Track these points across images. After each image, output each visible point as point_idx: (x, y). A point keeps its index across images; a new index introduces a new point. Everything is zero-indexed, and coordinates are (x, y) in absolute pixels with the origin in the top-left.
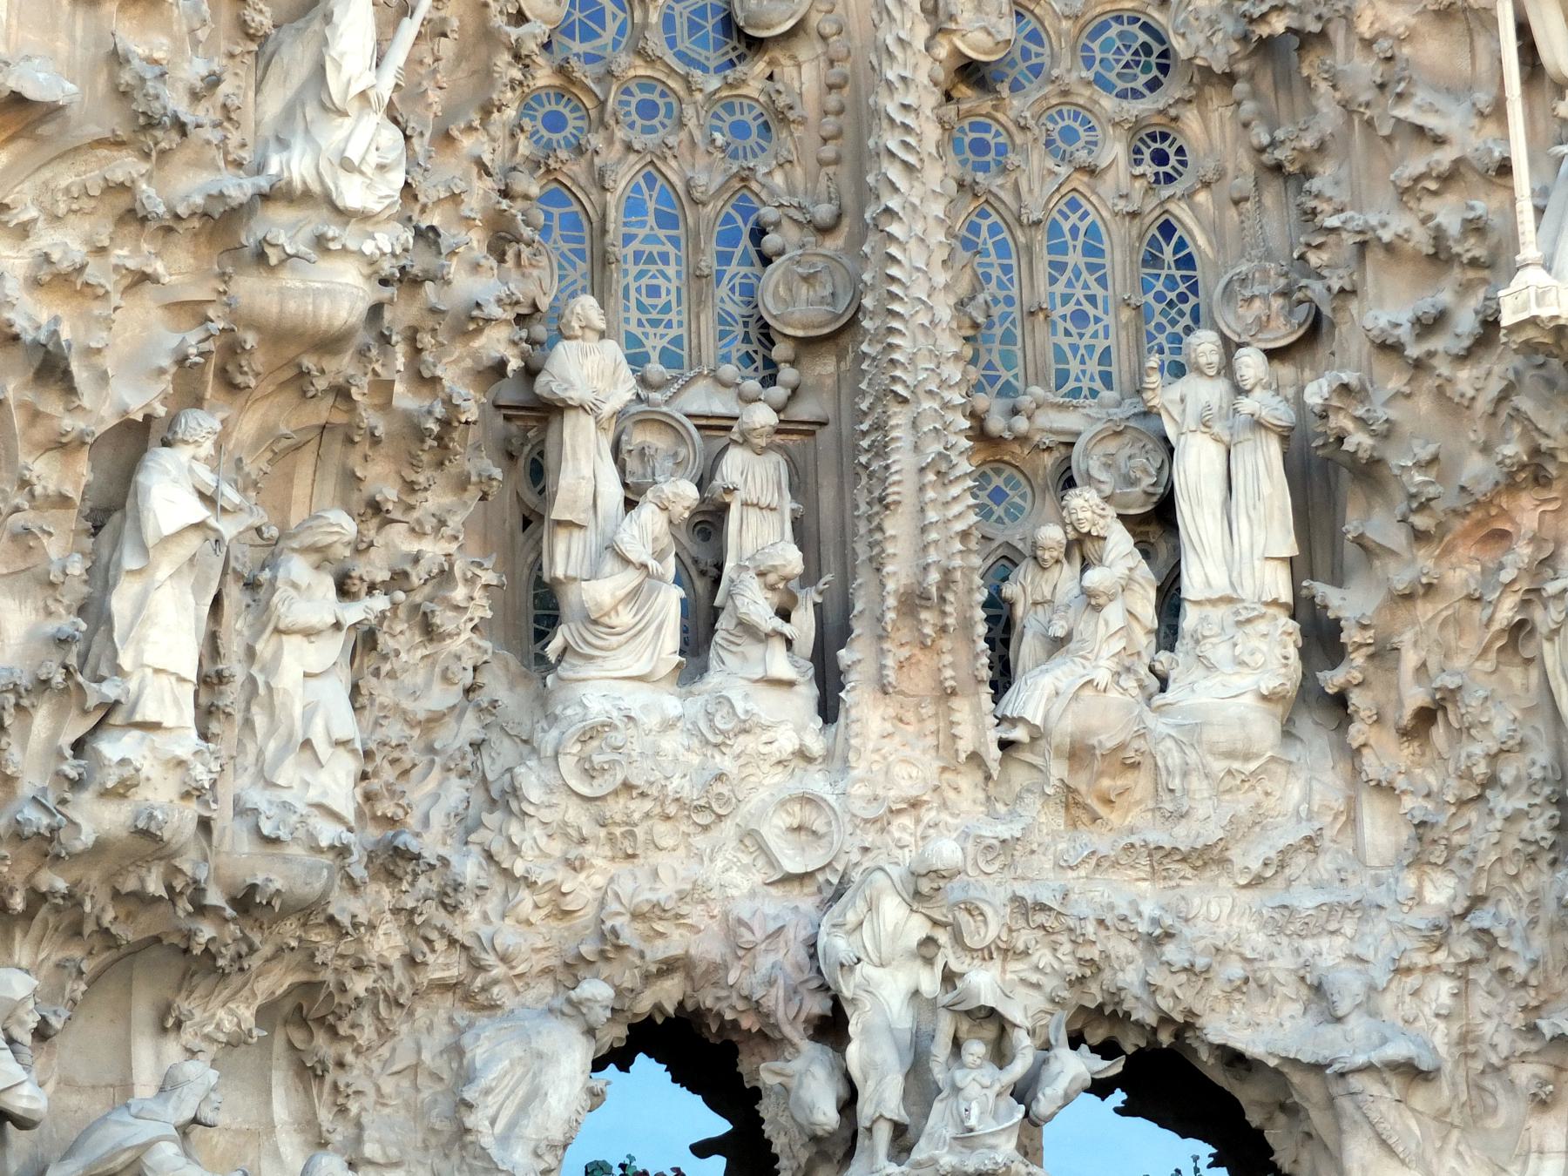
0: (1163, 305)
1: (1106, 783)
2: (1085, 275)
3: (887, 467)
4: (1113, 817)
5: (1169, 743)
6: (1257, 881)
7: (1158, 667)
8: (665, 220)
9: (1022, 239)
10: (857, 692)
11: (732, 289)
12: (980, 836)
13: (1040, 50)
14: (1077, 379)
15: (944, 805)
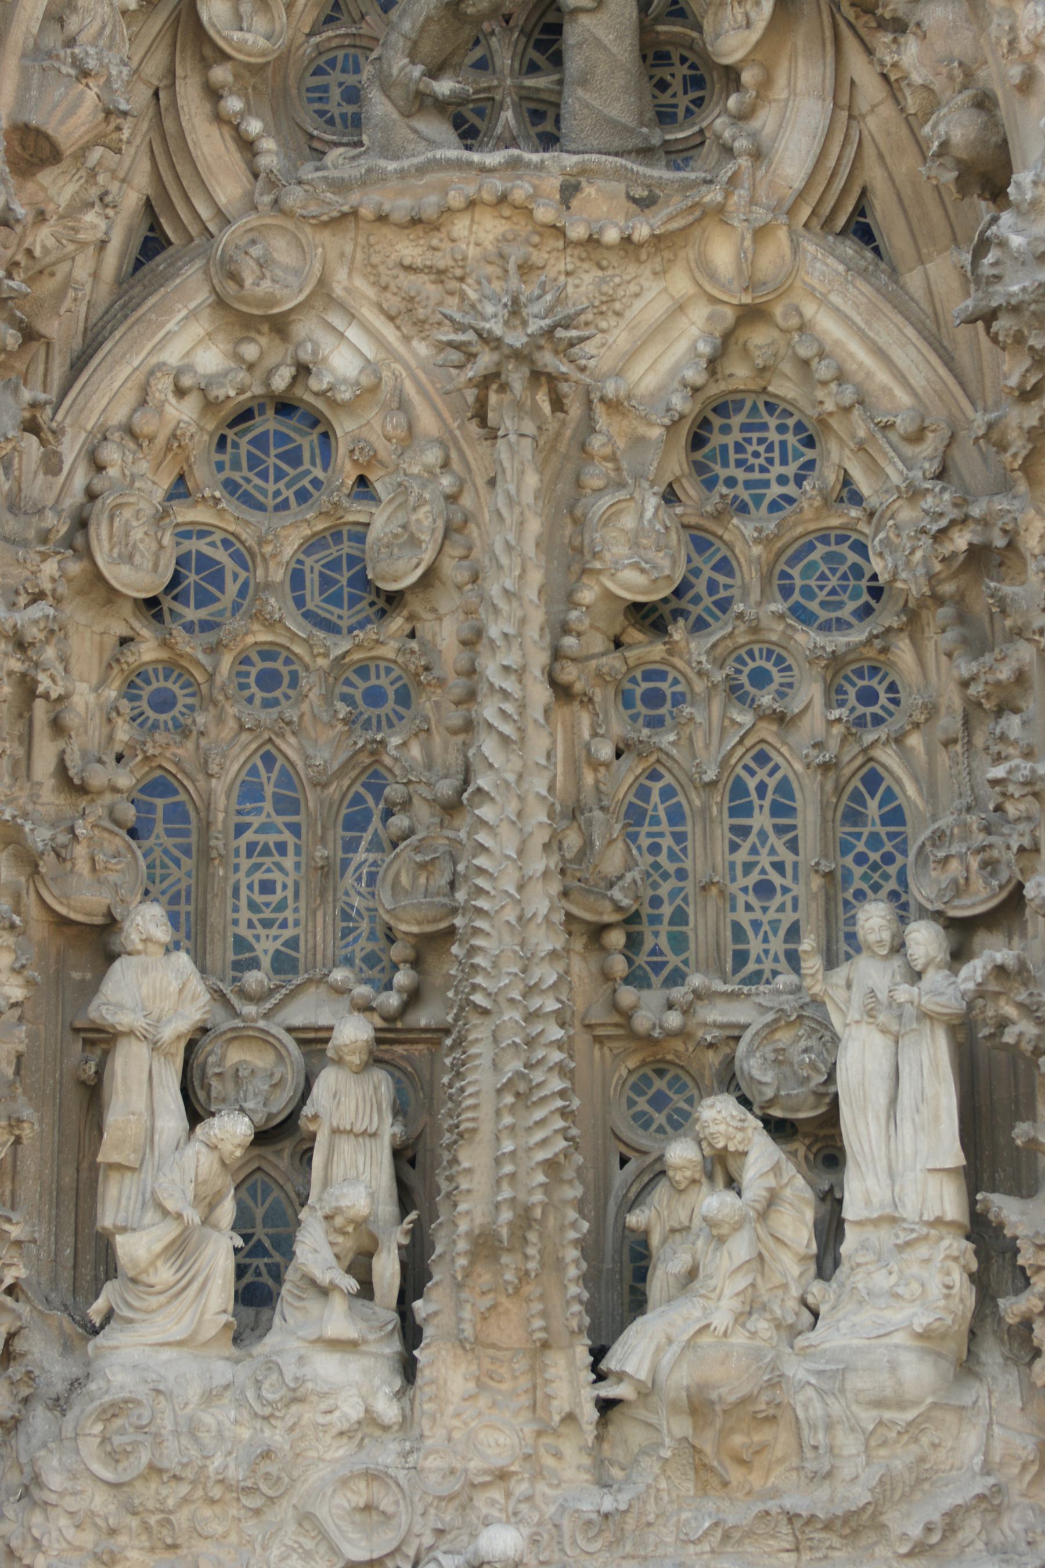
0: (864, 868)
1: (738, 1440)
2: (773, 838)
3: (462, 1090)
4: (756, 1480)
5: (810, 1392)
6: (919, 1550)
7: (810, 1300)
8: (287, 805)
9: (697, 802)
10: (433, 1349)
11: (359, 879)
12: (577, 1511)
13: (729, 581)
14: (759, 960)
15: (538, 1474)
